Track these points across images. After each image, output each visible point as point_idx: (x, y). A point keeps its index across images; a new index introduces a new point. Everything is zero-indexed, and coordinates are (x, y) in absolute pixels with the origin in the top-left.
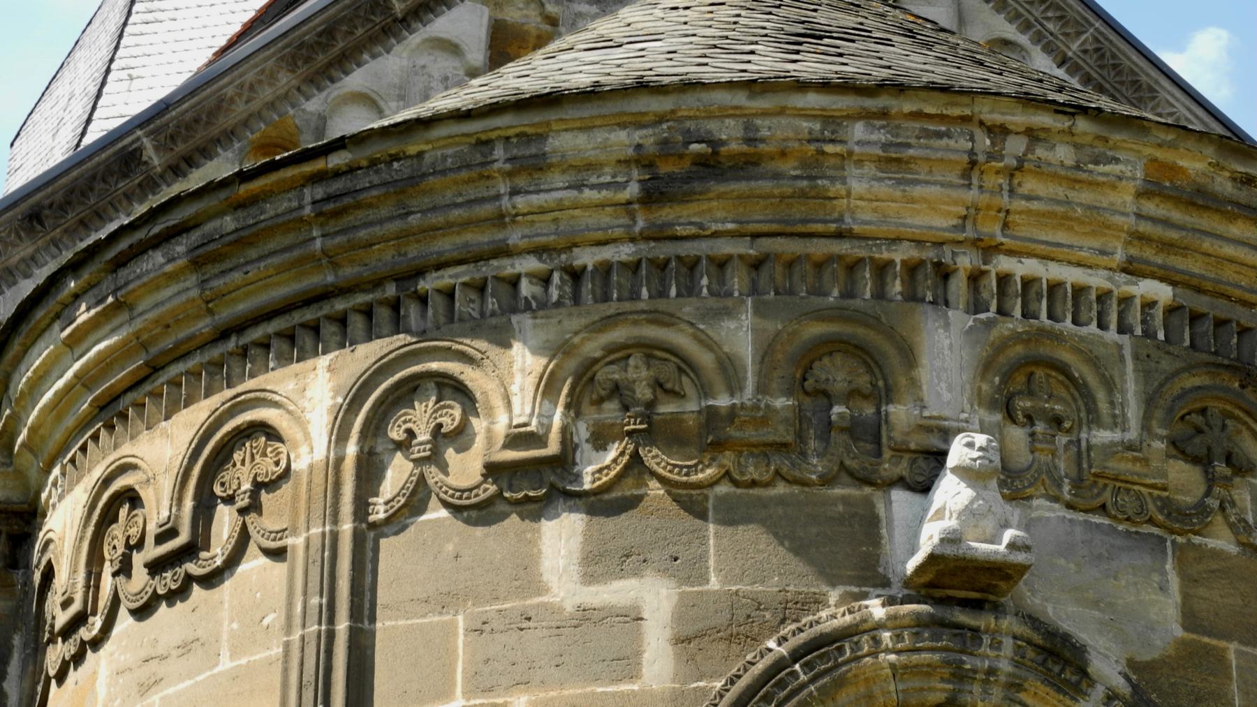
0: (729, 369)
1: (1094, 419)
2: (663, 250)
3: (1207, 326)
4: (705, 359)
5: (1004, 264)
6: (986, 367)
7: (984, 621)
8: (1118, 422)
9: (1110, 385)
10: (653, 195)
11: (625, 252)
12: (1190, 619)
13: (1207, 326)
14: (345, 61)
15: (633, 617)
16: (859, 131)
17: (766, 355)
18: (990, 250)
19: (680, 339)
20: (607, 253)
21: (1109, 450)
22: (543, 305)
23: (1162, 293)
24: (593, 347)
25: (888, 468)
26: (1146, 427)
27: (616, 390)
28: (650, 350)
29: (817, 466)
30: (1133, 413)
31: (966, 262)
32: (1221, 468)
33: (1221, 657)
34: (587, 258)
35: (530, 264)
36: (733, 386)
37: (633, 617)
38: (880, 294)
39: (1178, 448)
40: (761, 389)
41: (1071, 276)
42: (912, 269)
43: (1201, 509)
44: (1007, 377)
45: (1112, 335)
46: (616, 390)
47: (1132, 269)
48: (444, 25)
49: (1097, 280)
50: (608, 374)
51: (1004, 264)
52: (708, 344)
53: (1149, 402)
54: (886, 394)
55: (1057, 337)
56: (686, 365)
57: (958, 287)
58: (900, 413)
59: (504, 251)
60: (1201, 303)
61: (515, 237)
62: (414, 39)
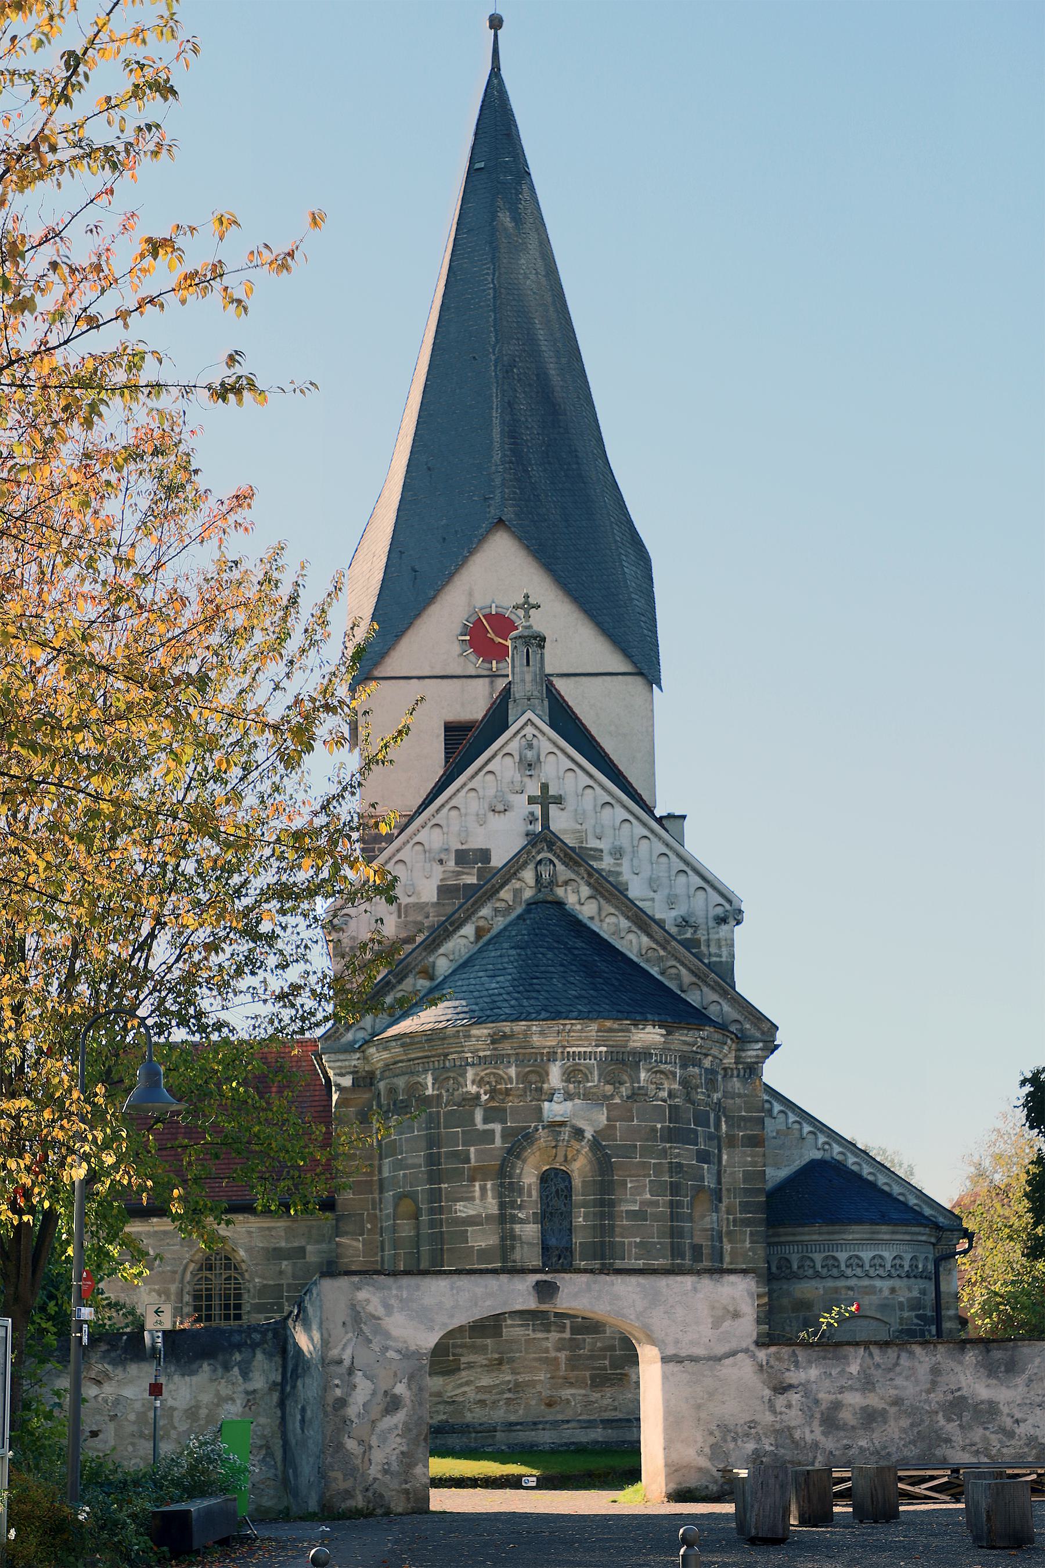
0: (510, 1079)
1: (588, 1081)
2: (497, 1052)
3: (614, 1054)
4: (505, 1077)
5: (568, 1049)
6: (564, 1074)
7: (563, 1129)
8: (593, 1081)
9: (591, 1073)
10: (493, 1042)
11: (488, 1053)
12: (608, 1119)
13: (614, 1054)
14: (439, 946)
15: (493, 1131)
16: (534, 1028)
17: (518, 1075)
18: (564, 1047)
19: (500, 1072)
20: (485, 1053)
21: (590, 1087)
22: (473, 1064)
23: (604, 1049)
24: (483, 1074)
25: (543, 1098)
26: (599, 1081)
27: (488, 1083)
28: (494, 1074)
29: (529, 1099)
30: (596, 1079)
31: (559, 1051)
32: (617, 1085)
33: (615, 1126)
34: (481, 1054)
35: (470, 1055)
36: (511, 1083)
37: (493, 1131)
38: (542, 1060)
39: (608, 1083)
40: (517, 1083)
41: (582, 1049)
42: (548, 1053)
43: (612, 1095)
44: (569, 1075)
45: (593, 1061)
46: (488, 1083)
47: (597, 1046)
48: (463, 931)
49: (589, 1050)
50: (487, 1079)
51: (568, 1049)
52: (506, 1074)
53: (600, 1075)
54: (543, 1083)
55: (579, 1064)
56: (502, 1078)
57: (559, 1056)
58: (545, 1086)
59: (463, 1052)
60: (613, 1049)
61: (466, 1049)
62: (456, 937)
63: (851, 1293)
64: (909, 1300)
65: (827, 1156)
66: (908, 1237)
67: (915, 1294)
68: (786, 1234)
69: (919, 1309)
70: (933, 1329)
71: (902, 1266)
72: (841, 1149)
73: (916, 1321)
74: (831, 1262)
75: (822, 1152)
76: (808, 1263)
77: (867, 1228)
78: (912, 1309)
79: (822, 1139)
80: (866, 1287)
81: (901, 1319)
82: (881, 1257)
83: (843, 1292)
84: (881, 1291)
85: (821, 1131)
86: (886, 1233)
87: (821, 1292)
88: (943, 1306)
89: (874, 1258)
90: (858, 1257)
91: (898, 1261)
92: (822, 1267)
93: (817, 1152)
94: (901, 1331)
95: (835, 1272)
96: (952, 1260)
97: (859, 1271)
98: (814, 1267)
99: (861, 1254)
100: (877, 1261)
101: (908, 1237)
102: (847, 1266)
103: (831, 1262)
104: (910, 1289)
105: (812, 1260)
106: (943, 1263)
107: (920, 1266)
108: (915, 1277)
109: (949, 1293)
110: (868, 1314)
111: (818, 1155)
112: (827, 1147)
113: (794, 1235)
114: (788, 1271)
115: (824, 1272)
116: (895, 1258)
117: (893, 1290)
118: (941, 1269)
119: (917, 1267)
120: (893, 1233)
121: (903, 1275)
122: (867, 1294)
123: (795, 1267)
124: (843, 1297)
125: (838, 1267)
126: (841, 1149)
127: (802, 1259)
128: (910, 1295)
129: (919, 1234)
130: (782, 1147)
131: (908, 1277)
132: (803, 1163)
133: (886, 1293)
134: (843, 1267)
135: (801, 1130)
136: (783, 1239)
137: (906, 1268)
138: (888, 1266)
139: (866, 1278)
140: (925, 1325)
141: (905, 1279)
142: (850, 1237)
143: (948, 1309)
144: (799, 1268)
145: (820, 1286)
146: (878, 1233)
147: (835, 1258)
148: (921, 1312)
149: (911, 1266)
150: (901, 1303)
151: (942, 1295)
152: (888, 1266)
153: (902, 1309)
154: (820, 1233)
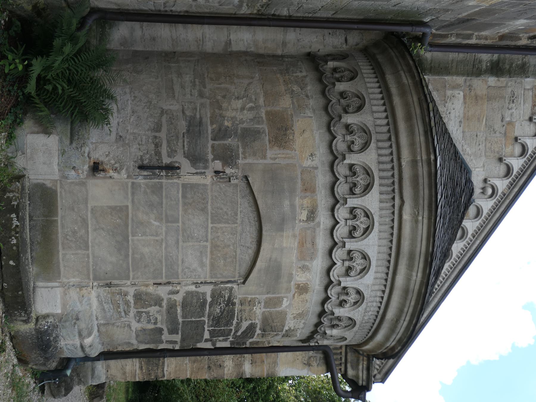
63: (304, 216)
64: (283, 315)
65: (477, 191)
66: (391, 314)
67: (290, 324)
68: (407, 106)
69: (264, 330)
70: (227, 344)
71: (341, 304)
72: (485, 211)
73: (245, 325)
74: (361, 180)
75: (481, 185)
76: (359, 142)
77: (421, 247)
78: (265, 320)
79: (502, 185)
80: (313, 244)
81: (252, 303)
82: (364, 270)
83: (306, 202)
84: (305, 268)
85: (511, 186)
86: (408, 279)
87: (308, 163)
88: (257, 356)
89: (365, 257)
90: (367, 230)
91: (352, 297)
92: (351, 167)
93: (482, 178)
94: (230, 302)
95: (342, 189)
96: (324, 368)
97: (341, 231)
98: (350, 150)
99: (374, 235)
100: (358, 264)
101: (391, 314)
102: (352, 210)
103: (361, 180)
104: (300, 316)
105: (365, 146)
106: (319, 355)
107: (335, 332)
108: (319, 324)
109: (275, 363)
110: (265, 246)
111: (477, 180)
112: (490, 191)
113: (409, 118)
114: (339, 109)
115: (342, 170)
116: (359, 292)
117: (303, 289)
118: (311, 353)
119: (333, 326)
120: (406, 291)
121: (328, 307)
122: (302, 244)
123: (350, 119)
124: (297, 201)
125: (352, 192)
126: (485, 211)
127: (365, 131)
128: (289, 316)
129: (393, 329)
130: (490, 128)
131: (322, 313)
132: (467, 159)
133: (300, 278)
134: (352, 202)
135: (512, 156)
136: (397, 101)
137: (339, 312)
138: (347, 282)
139: (329, 243)
140: (235, 337)
141: (318, 309)
142: (406, 217)
143: (253, 362)
144: (347, 127)
145: (316, 162)
146: (410, 266)
147: (368, 188)
148: (258, 331)
149: (339, 319)
150: (278, 302)
151: (273, 355)
152: (347, 282)
153: (268, 303)
154: (414, 163)
